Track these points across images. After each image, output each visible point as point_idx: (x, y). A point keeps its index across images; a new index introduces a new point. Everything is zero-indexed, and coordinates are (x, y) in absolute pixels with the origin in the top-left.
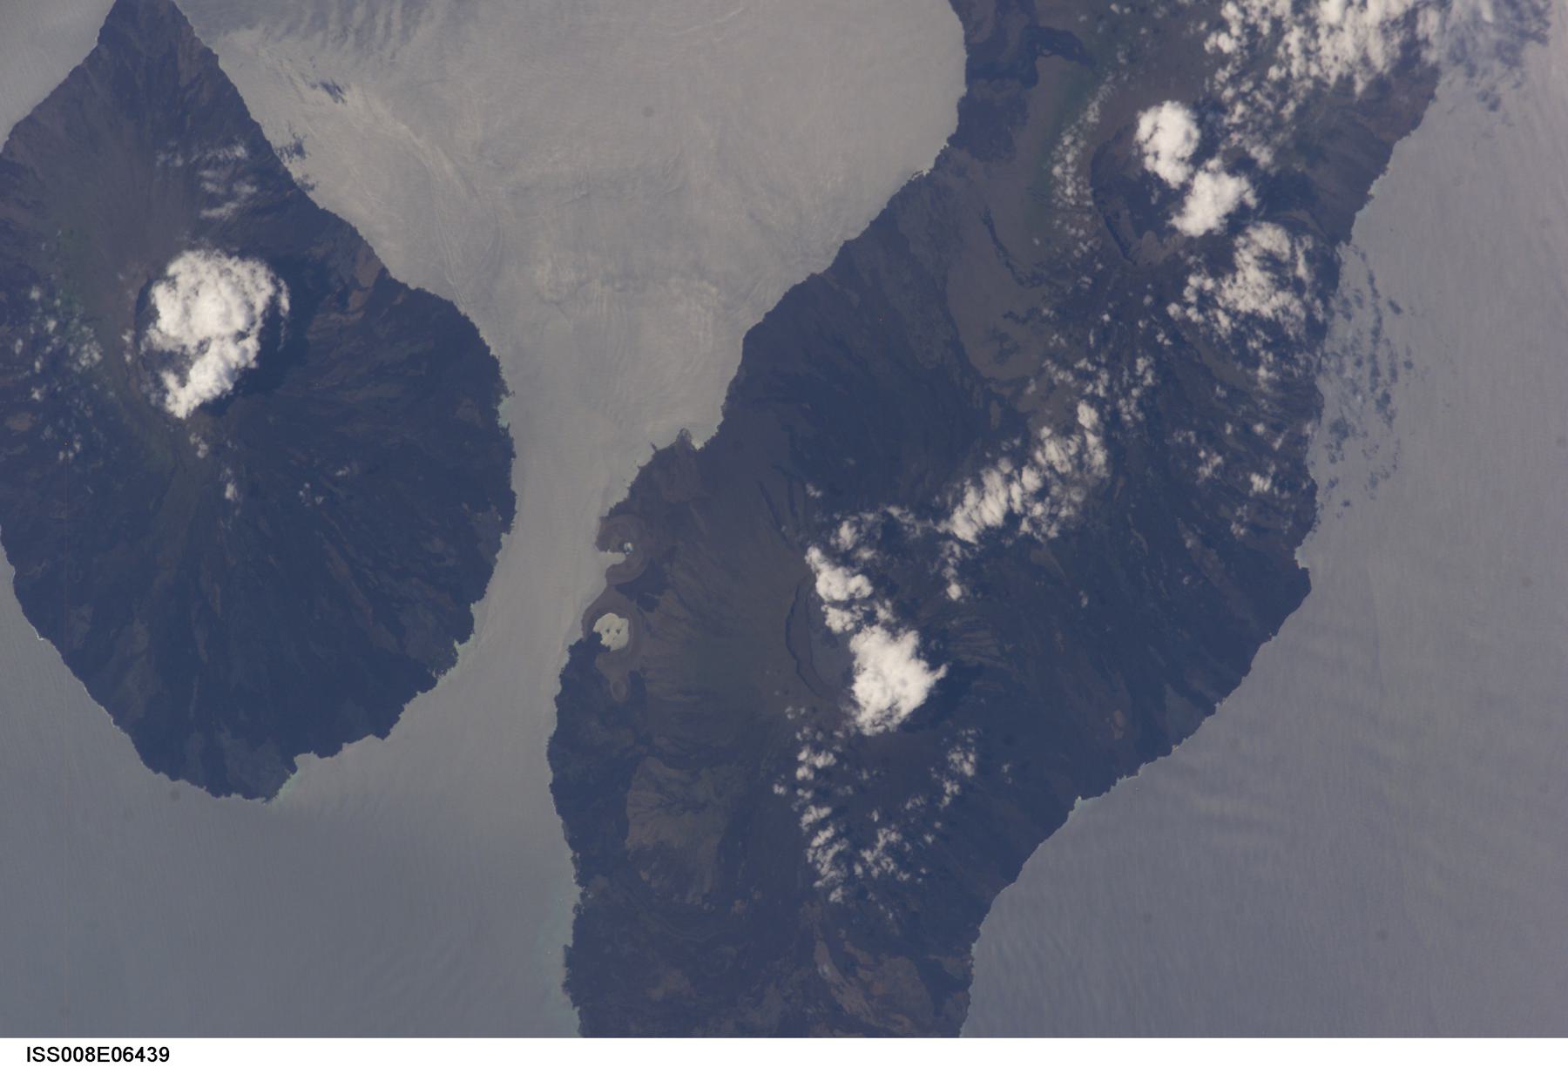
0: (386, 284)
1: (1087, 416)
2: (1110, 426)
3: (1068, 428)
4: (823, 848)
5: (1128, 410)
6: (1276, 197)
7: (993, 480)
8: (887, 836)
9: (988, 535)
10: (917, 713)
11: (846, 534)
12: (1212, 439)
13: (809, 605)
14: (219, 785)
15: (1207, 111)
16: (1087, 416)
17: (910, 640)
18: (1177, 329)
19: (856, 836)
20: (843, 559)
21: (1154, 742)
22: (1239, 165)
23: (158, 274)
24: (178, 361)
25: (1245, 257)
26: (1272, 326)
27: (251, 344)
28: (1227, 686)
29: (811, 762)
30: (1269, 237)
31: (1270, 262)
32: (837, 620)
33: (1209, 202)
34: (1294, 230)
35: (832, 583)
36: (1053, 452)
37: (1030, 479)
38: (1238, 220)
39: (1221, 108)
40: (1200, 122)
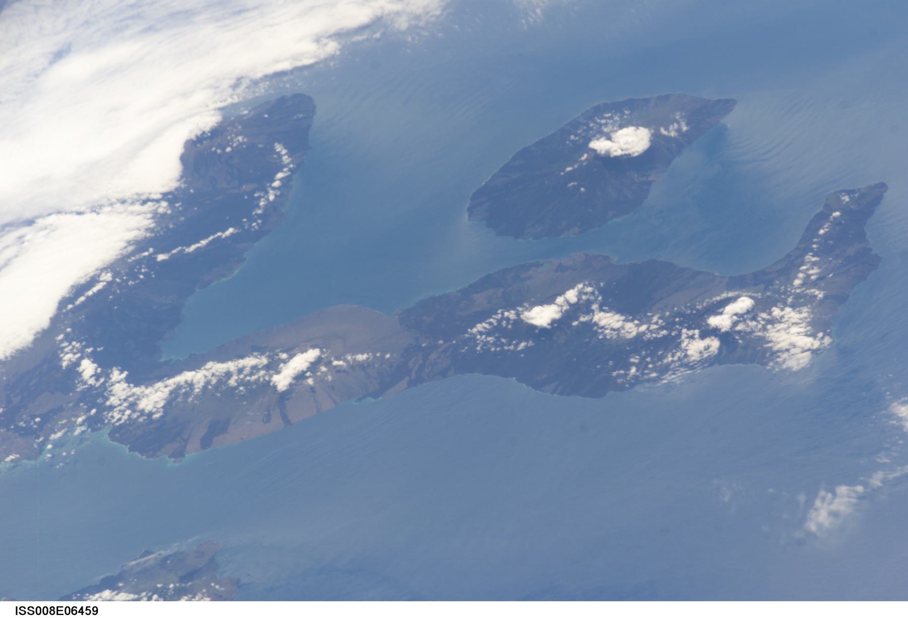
0: (649, 184)
1: (643, 328)
2: (640, 336)
3: (638, 326)
4: (480, 327)
5: (648, 336)
6: (726, 338)
7: (617, 317)
8: (491, 339)
9: (596, 324)
10: (533, 327)
11: (589, 289)
12: (643, 359)
13: (562, 293)
14: (470, 210)
15: (752, 314)
16: (643, 328)
17: (557, 316)
18: (679, 335)
19: (488, 333)
20: (581, 293)
21: (538, 386)
22: (735, 324)
23: (637, 126)
24: (609, 138)
25: (707, 341)
26: (686, 356)
27: (619, 153)
28: (561, 394)
29: (511, 315)
30: (714, 344)
31: (707, 348)
32: (560, 300)
33: (722, 321)
34: (720, 349)
35: (571, 295)
36: (629, 325)
37: (617, 325)
38: (715, 332)
39: (754, 319)
40: (748, 312)
